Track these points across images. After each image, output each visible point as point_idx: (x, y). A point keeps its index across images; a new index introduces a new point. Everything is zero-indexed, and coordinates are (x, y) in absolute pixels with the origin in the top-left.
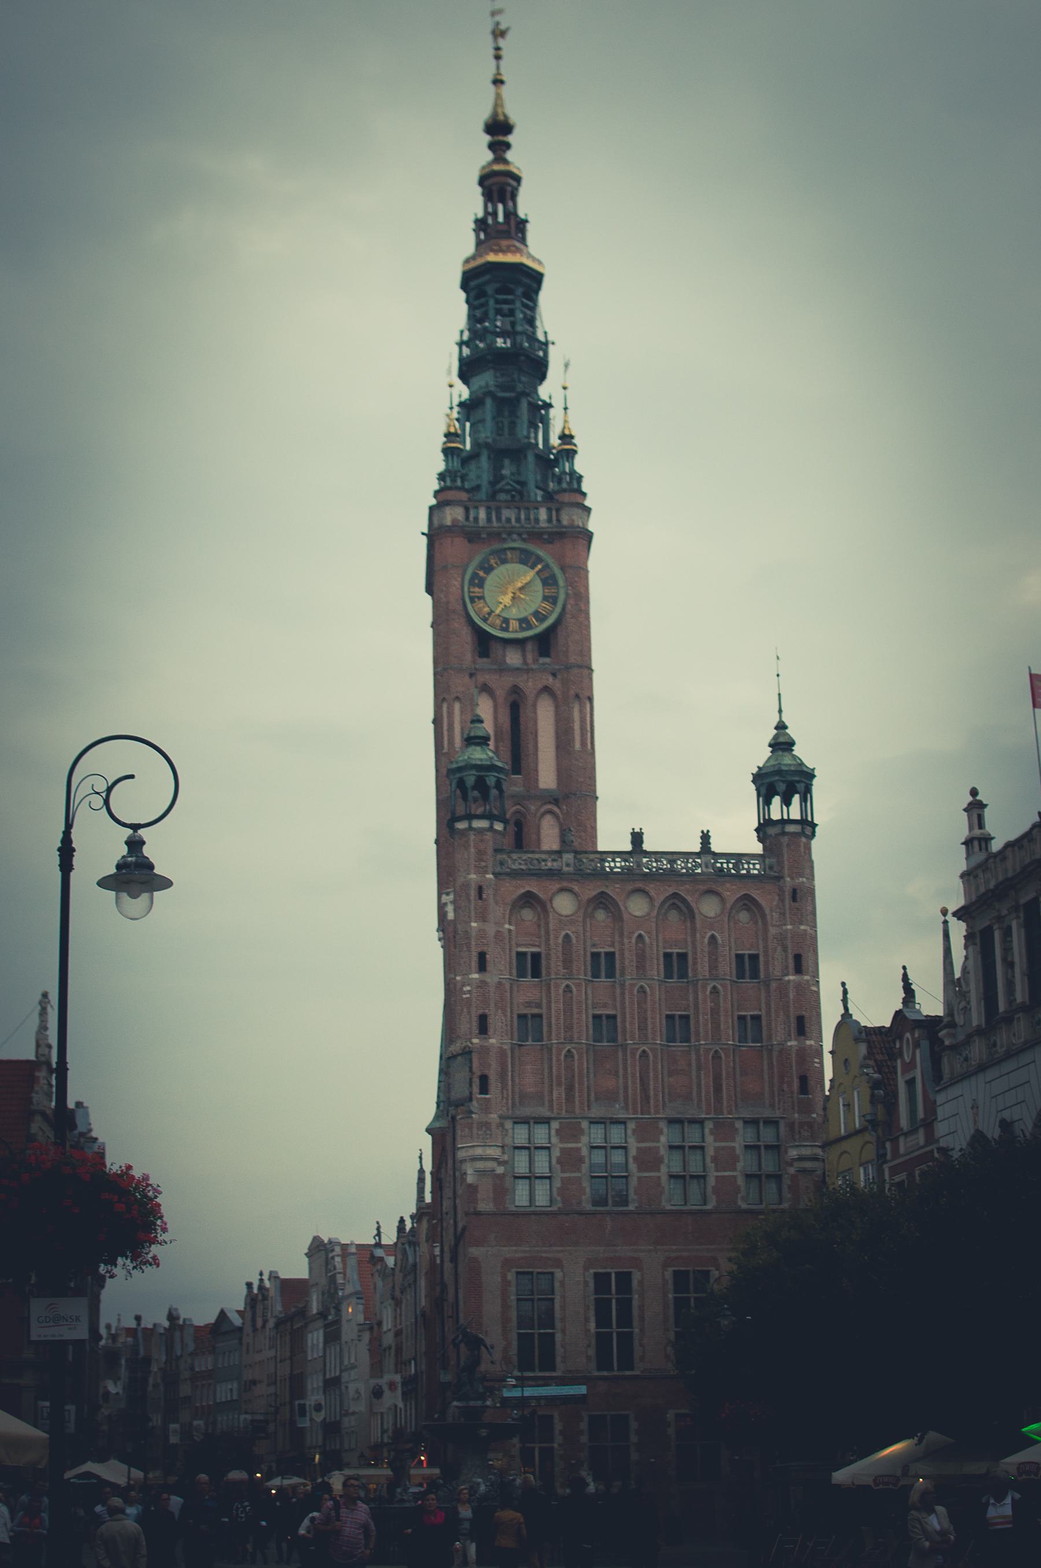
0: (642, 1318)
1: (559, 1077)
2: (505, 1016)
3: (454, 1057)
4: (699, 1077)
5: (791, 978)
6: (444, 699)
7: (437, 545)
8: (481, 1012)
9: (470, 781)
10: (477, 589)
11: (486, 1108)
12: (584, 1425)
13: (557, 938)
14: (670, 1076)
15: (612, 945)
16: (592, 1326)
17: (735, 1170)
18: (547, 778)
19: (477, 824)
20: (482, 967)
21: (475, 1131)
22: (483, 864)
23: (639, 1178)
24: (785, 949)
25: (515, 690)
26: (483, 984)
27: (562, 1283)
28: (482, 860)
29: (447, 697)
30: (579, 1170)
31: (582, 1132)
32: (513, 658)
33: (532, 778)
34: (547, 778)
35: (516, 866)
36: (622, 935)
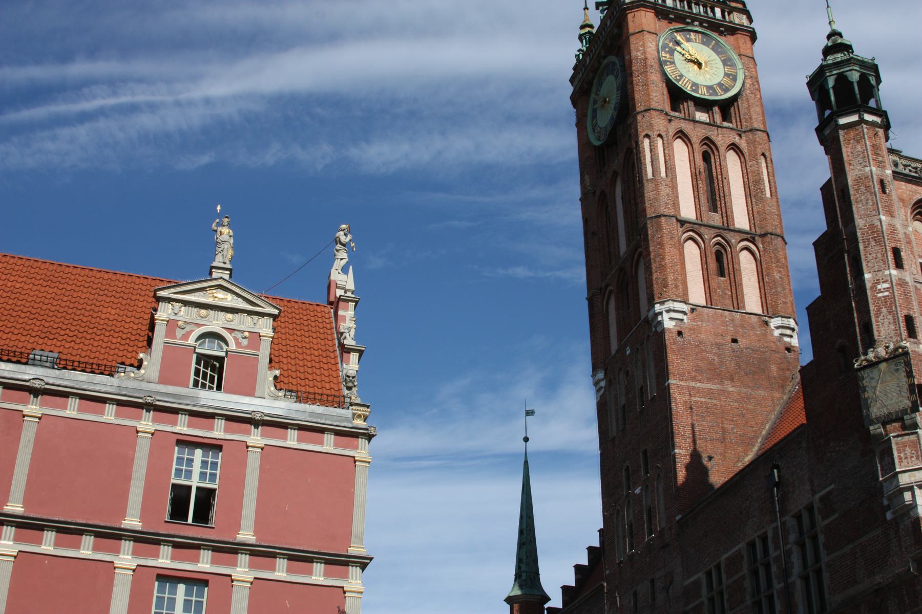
3: (872, 365)
6: (647, 136)
7: (630, 16)
8: (905, 312)
9: (855, 76)
10: (668, 56)
18: (741, 220)
19: (868, 117)
20: (899, 265)
22: (881, 159)
25: (708, 141)
29: (650, 133)
32: (701, 116)
33: (727, 215)
34: (741, 220)
35: (907, 171)
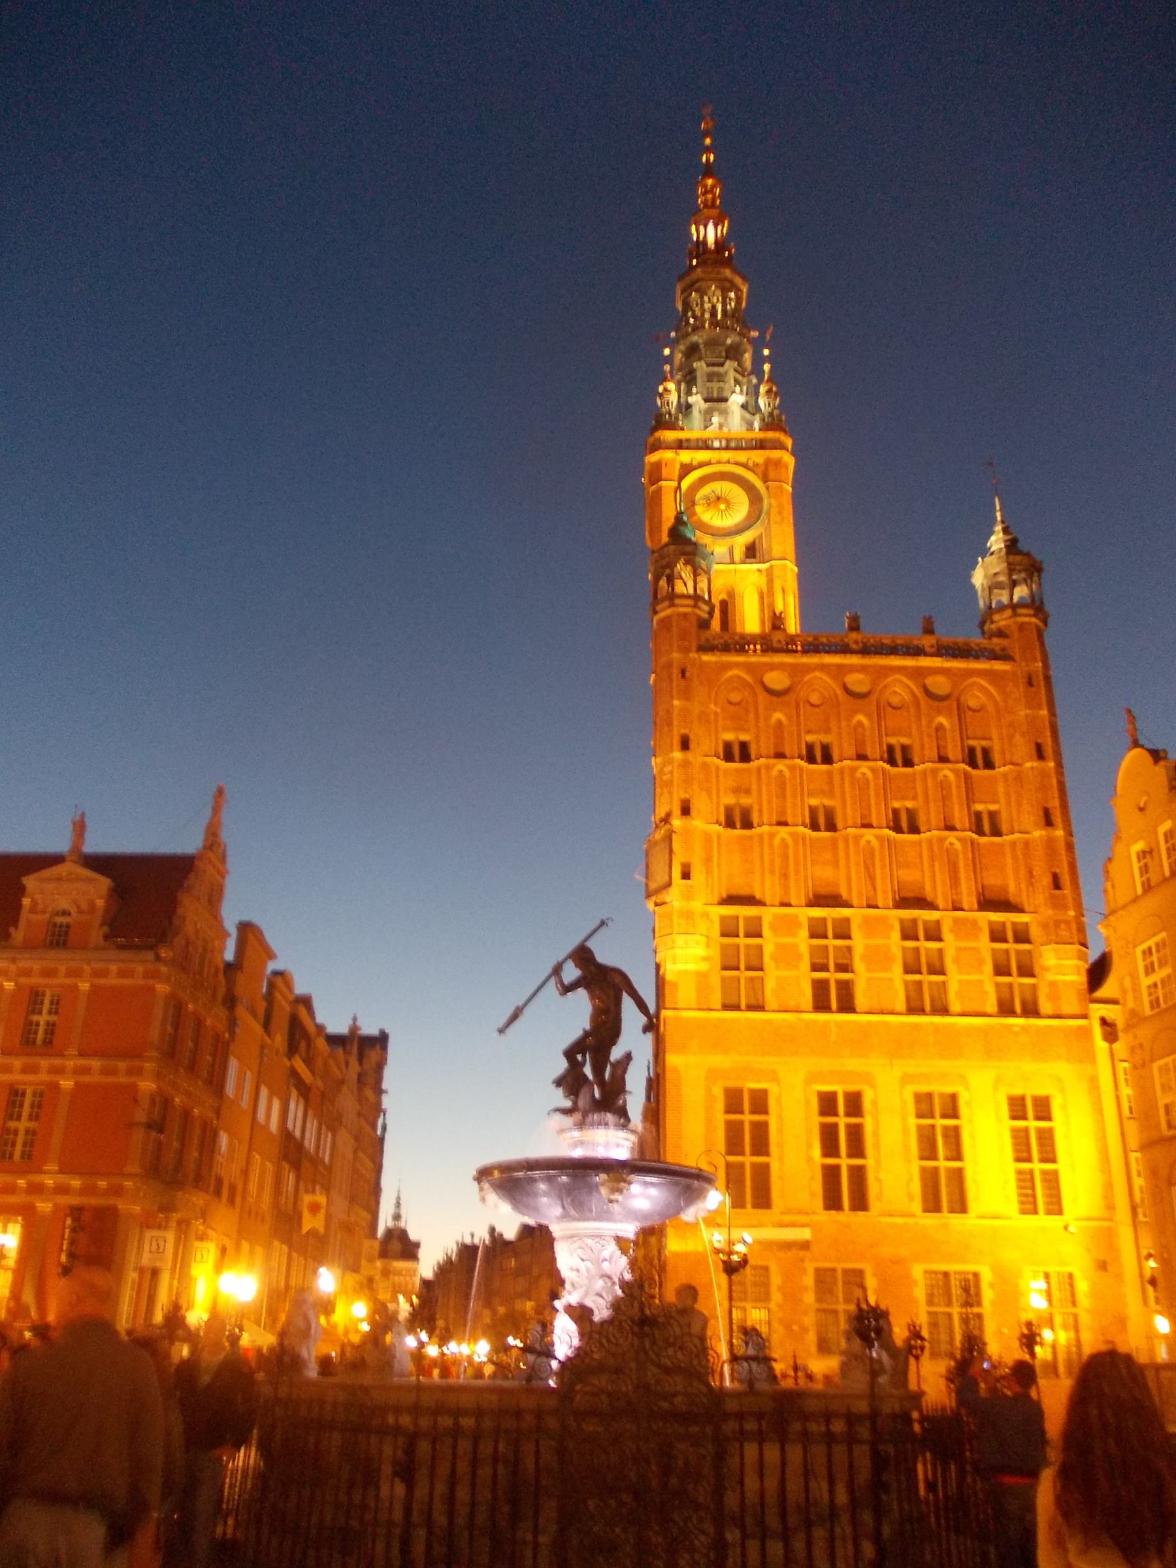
0: (877, 1146)
1: (772, 865)
2: (711, 799)
4: (932, 866)
5: (1035, 764)
11: (688, 896)
12: (809, 1280)
13: (768, 718)
14: (898, 868)
15: (827, 731)
16: (817, 1151)
17: (981, 972)
20: (685, 745)
21: (675, 919)
23: (869, 979)
24: (1023, 734)
26: (686, 764)
27: (779, 1100)
28: (684, 639)
30: (796, 967)
31: (799, 925)
36: (839, 720)
